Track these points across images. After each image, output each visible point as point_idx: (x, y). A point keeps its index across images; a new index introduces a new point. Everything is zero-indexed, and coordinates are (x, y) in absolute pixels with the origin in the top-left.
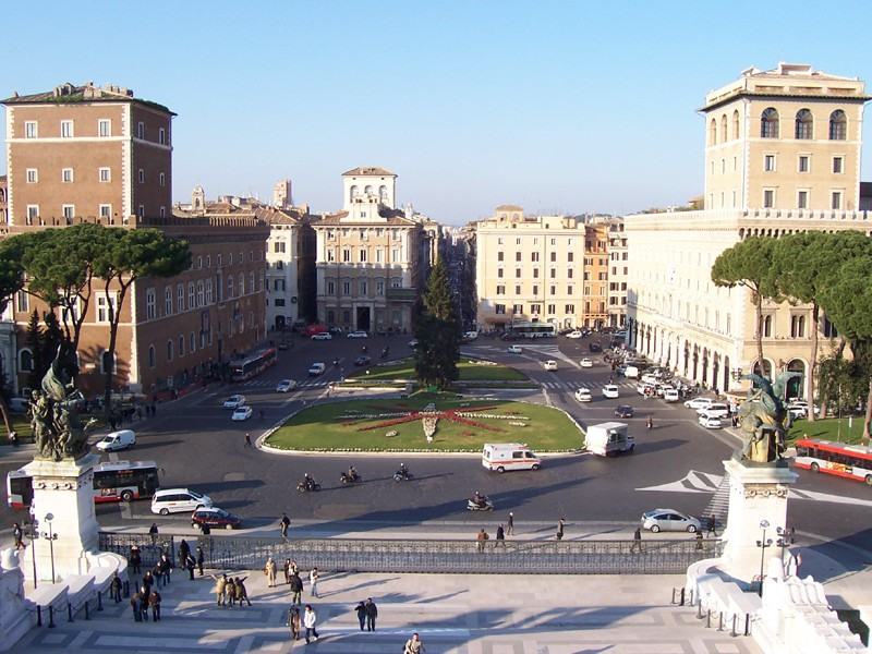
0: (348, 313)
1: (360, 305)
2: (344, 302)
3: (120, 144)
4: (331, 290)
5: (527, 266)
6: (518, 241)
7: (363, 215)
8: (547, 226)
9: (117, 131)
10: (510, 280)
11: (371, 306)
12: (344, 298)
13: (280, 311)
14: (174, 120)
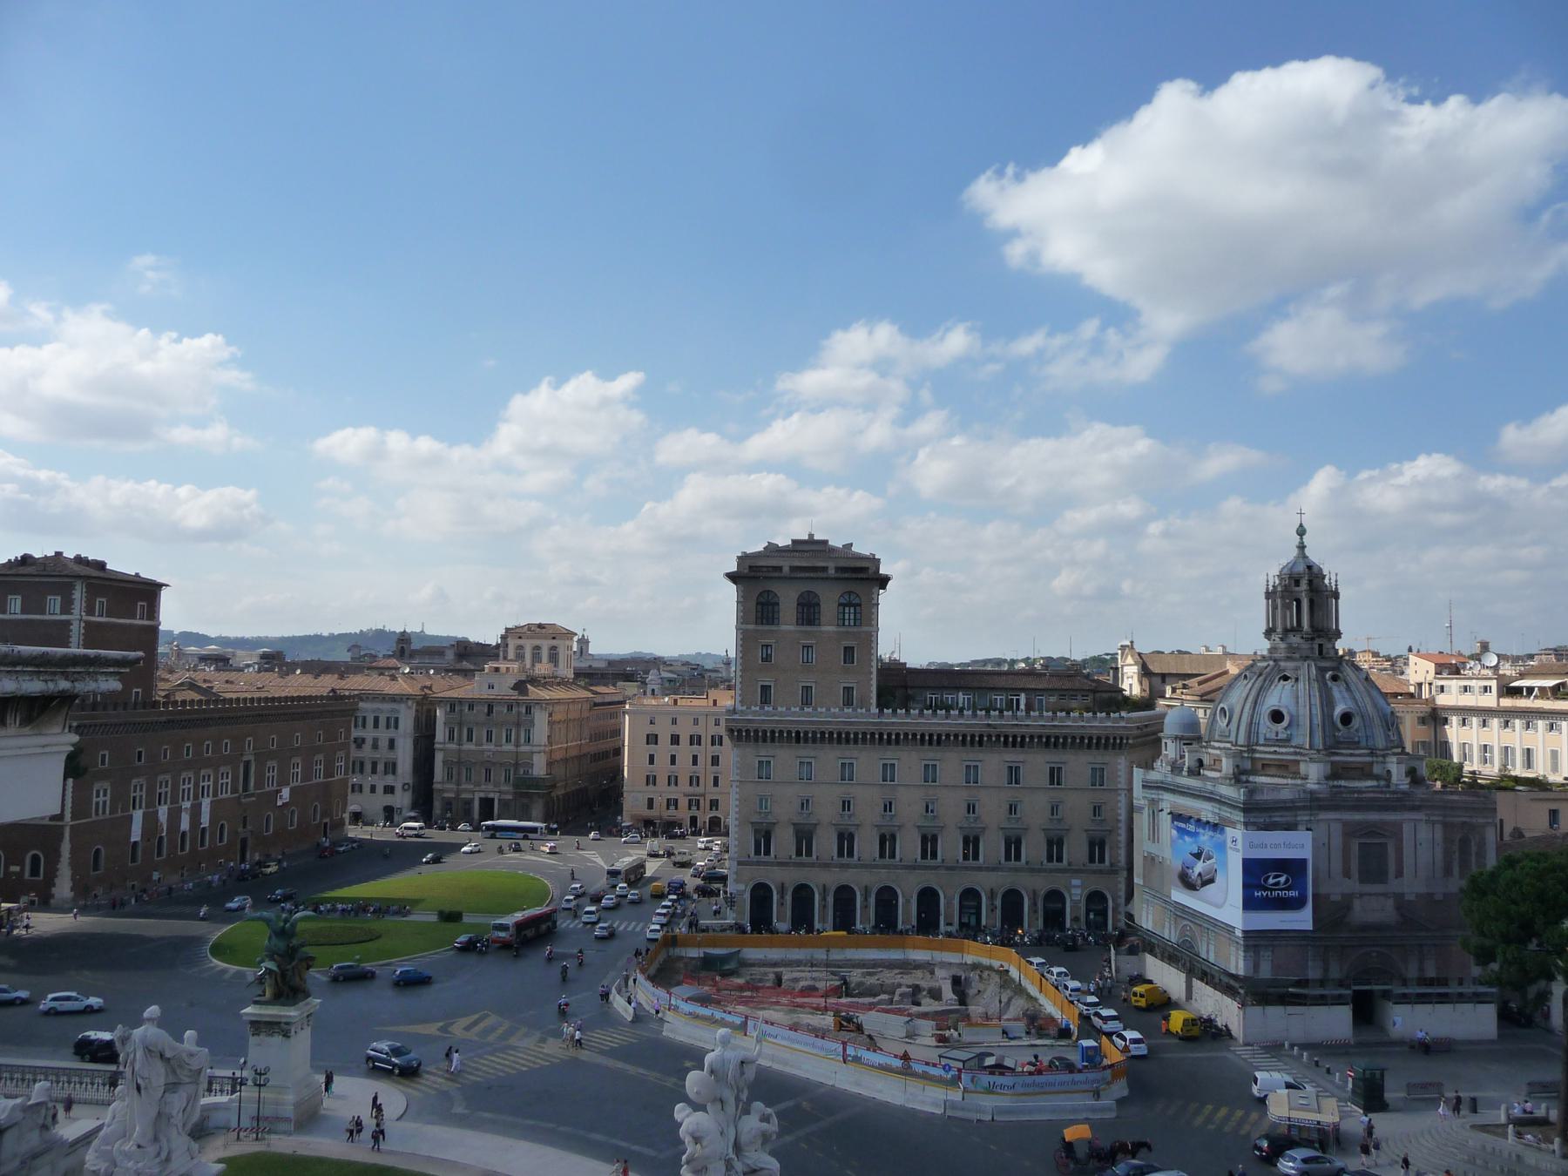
0: (469, 802)
1: (482, 795)
2: (466, 791)
3: (68, 623)
4: (450, 776)
5: (684, 751)
6: (674, 722)
7: (491, 687)
8: (715, 702)
9: (67, 608)
10: (662, 767)
11: (496, 797)
13: (389, 800)
14: (164, 593)
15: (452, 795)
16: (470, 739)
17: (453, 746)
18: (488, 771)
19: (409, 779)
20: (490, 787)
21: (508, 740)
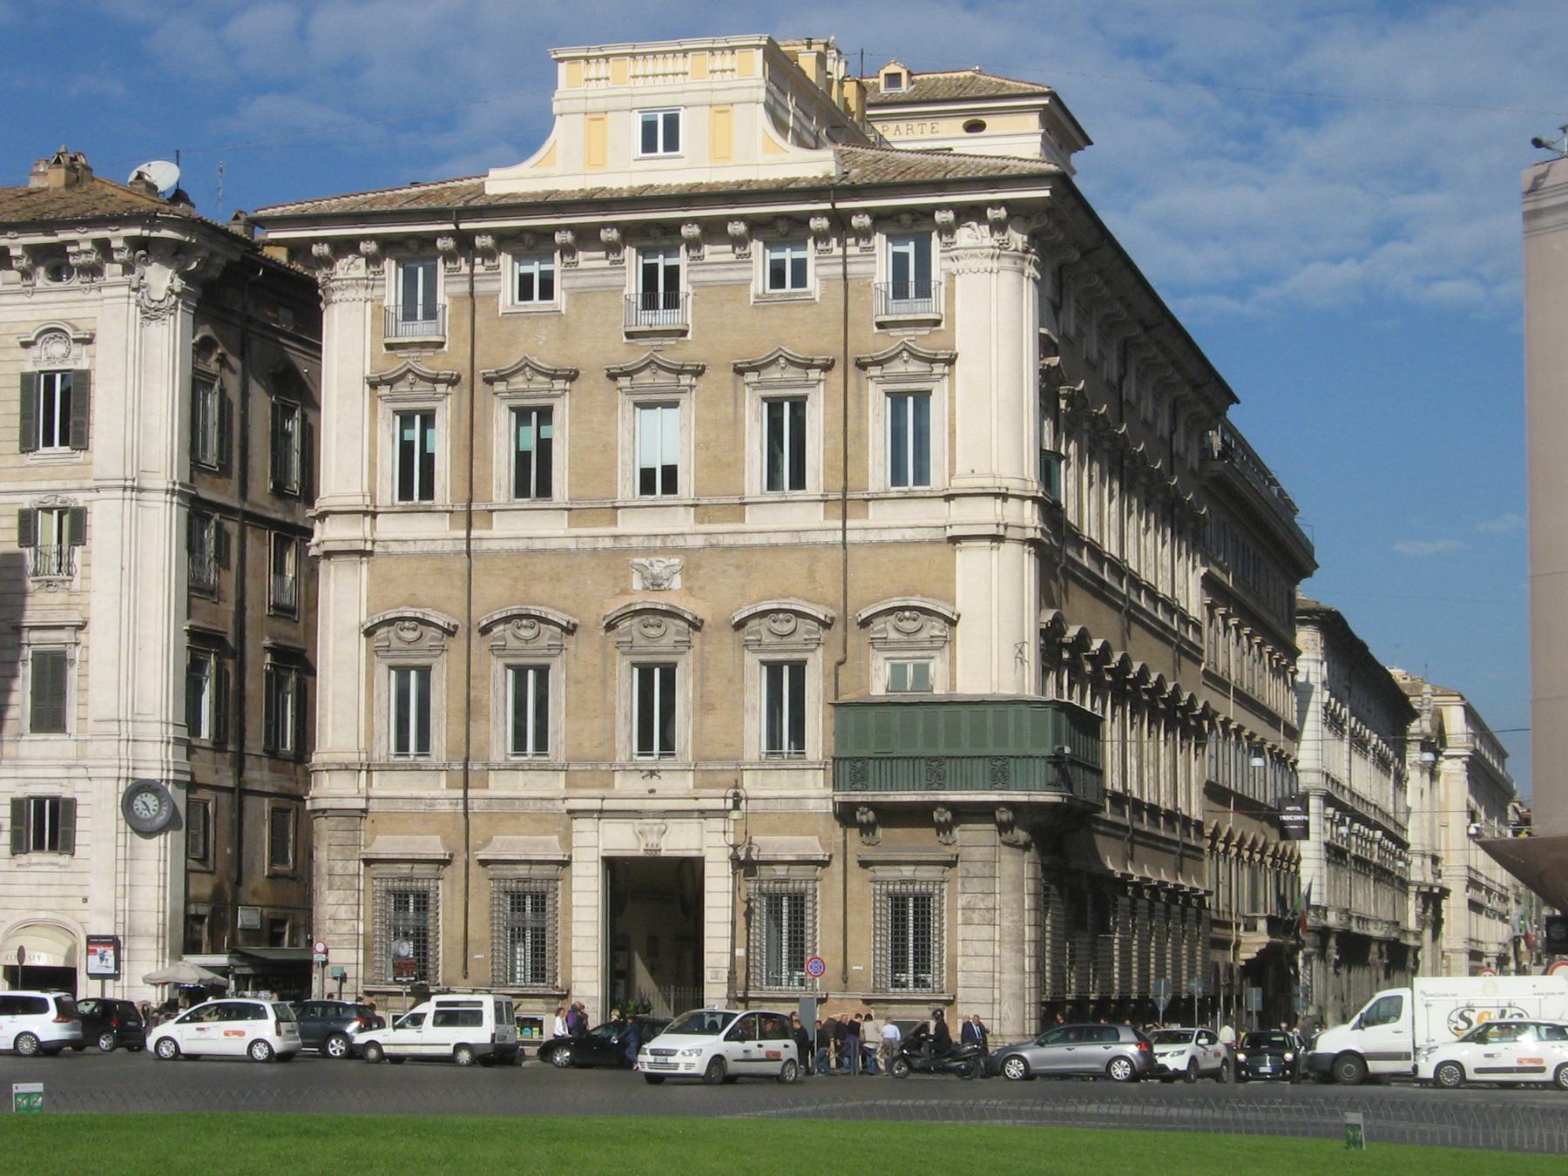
0: (529, 907)
1: (624, 839)
2: (510, 812)
4: (412, 729)
7: (661, 133)
12: (503, 786)
15: (434, 847)
16: (534, 475)
17: (430, 530)
18: (657, 687)
19: (157, 760)
20: (675, 785)
21: (787, 463)
